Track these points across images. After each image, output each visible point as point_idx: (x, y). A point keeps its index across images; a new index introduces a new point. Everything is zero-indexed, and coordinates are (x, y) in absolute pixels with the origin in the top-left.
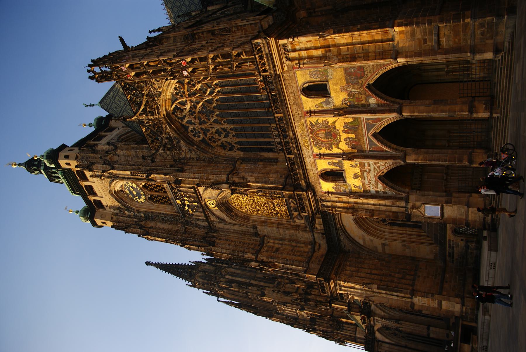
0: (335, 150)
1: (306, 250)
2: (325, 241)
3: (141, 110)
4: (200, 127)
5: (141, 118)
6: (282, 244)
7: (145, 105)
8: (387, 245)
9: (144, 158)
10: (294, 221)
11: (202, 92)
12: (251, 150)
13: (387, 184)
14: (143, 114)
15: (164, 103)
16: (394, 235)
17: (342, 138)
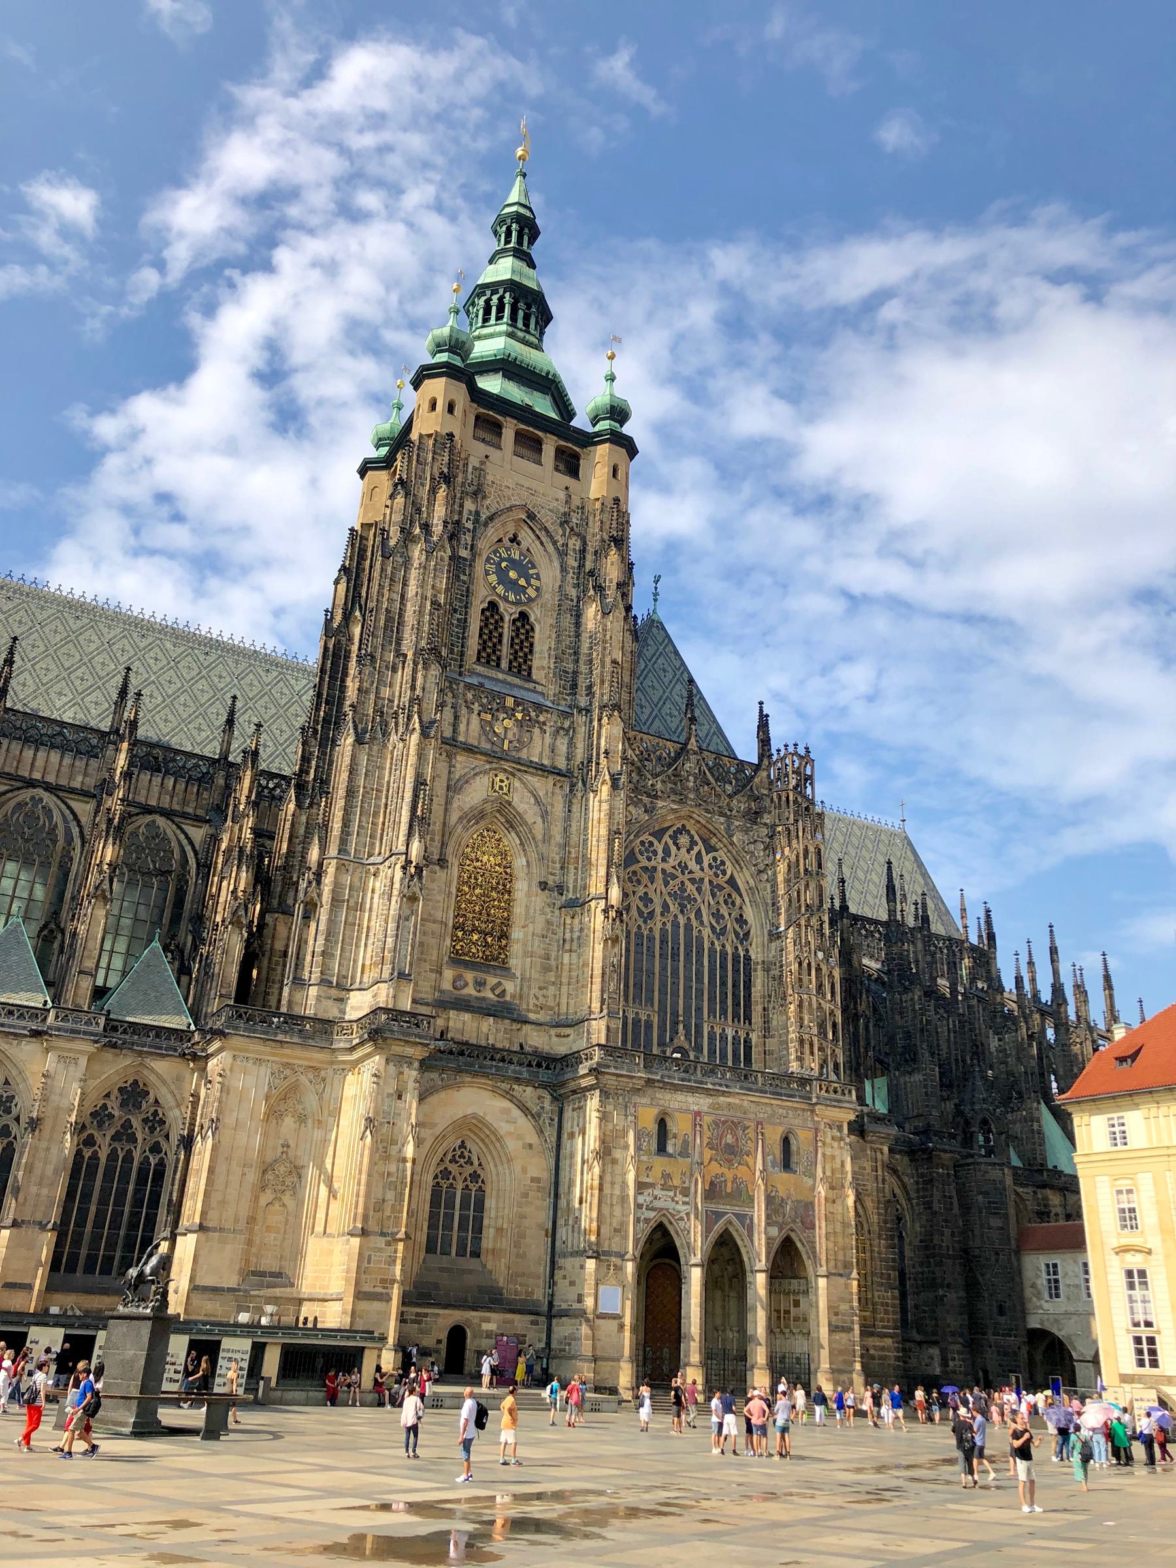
15: (710, 827)
17: (725, 1171)
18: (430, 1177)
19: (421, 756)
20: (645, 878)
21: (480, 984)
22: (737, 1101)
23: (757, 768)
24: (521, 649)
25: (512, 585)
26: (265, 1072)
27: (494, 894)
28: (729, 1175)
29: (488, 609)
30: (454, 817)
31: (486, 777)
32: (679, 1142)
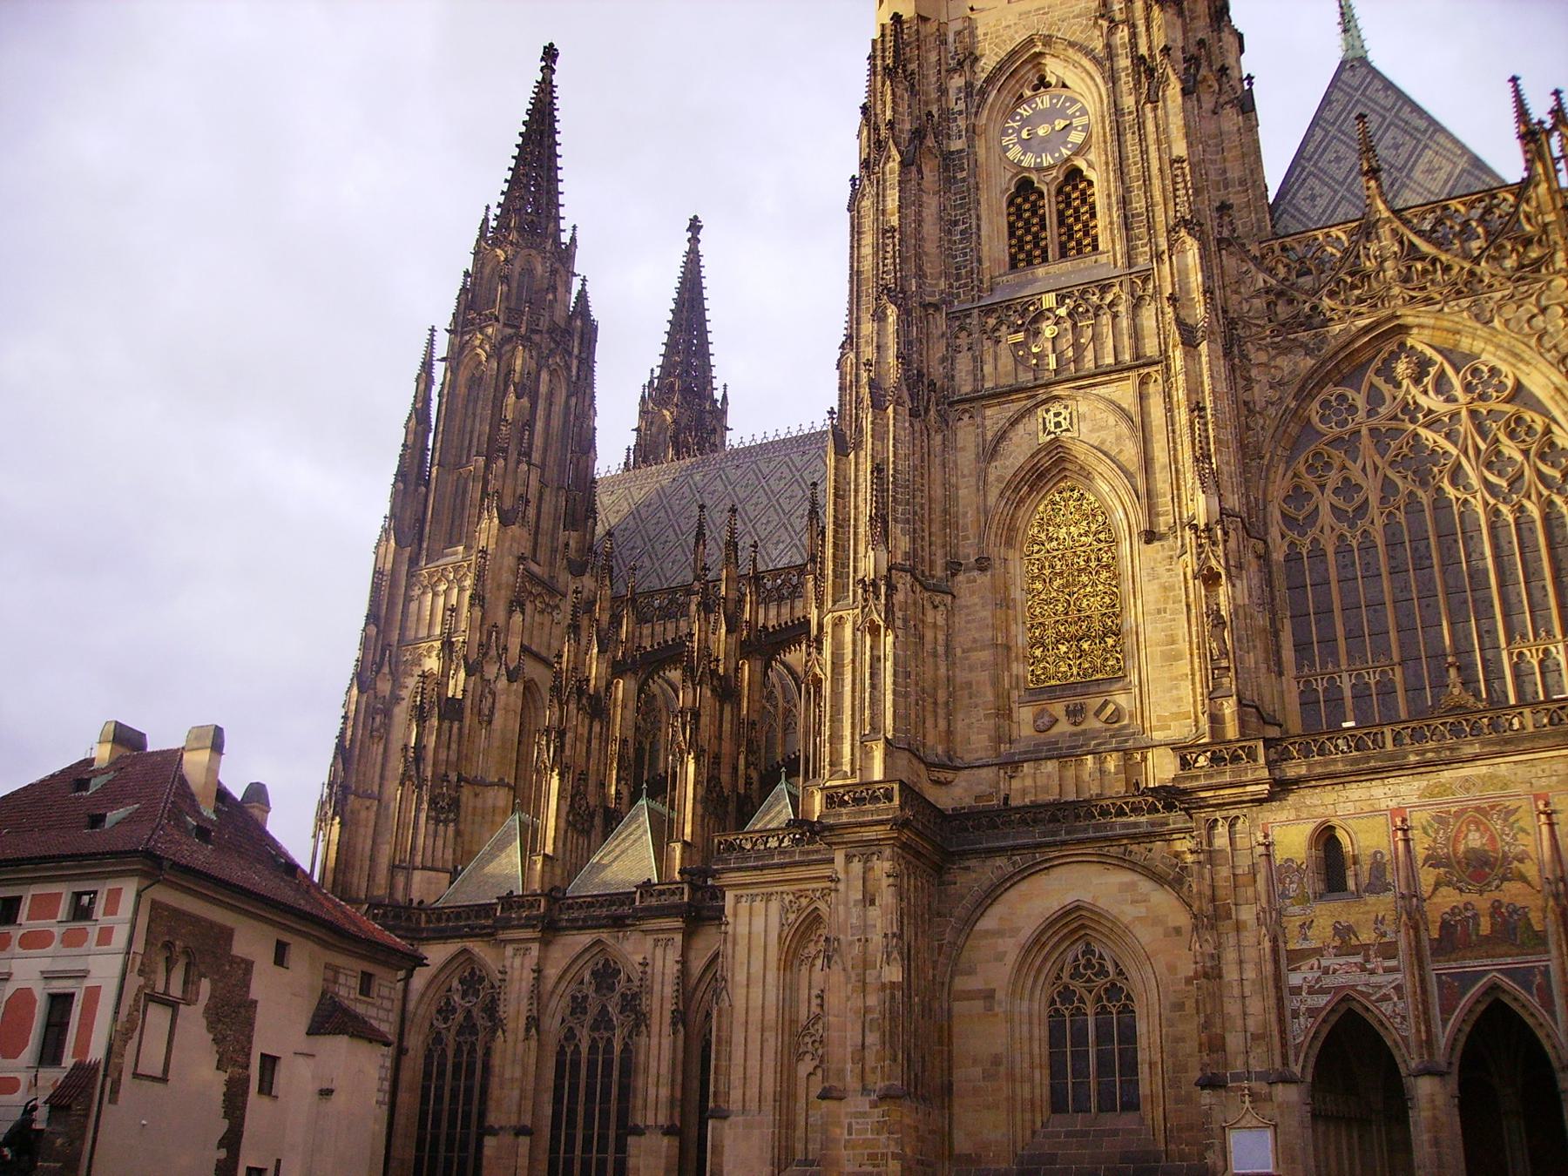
0: (1427, 877)
1: (931, 740)
2: (968, 801)
3: (1416, 240)
4: (1364, 431)
5: (1385, 231)
6: (935, 655)
7: (1434, 261)
8: (991, 1009)
9: (1224, 208)
10: (1022, 703)
11: (1493, 460)
12: (1296, 587)
13: (1324, 1021)
14: (1401, 243)
15: (1446, 324)
16: (1025, 1028)
17: (1473, 897)
18: (1034, 1006)
19: (879, 435)
20: (1338, 456)
21: (1075, 713)
22: (1484, 770)
23: (1522, 190)
24: (1077, 220)
25: (1045, 145)
26: (774, 906)
27: (1084, 579)
28: (1483, 903)
29: (1018, 193)
30: (992, 499)
31: (1033, 420)
32: (1366, 867)
